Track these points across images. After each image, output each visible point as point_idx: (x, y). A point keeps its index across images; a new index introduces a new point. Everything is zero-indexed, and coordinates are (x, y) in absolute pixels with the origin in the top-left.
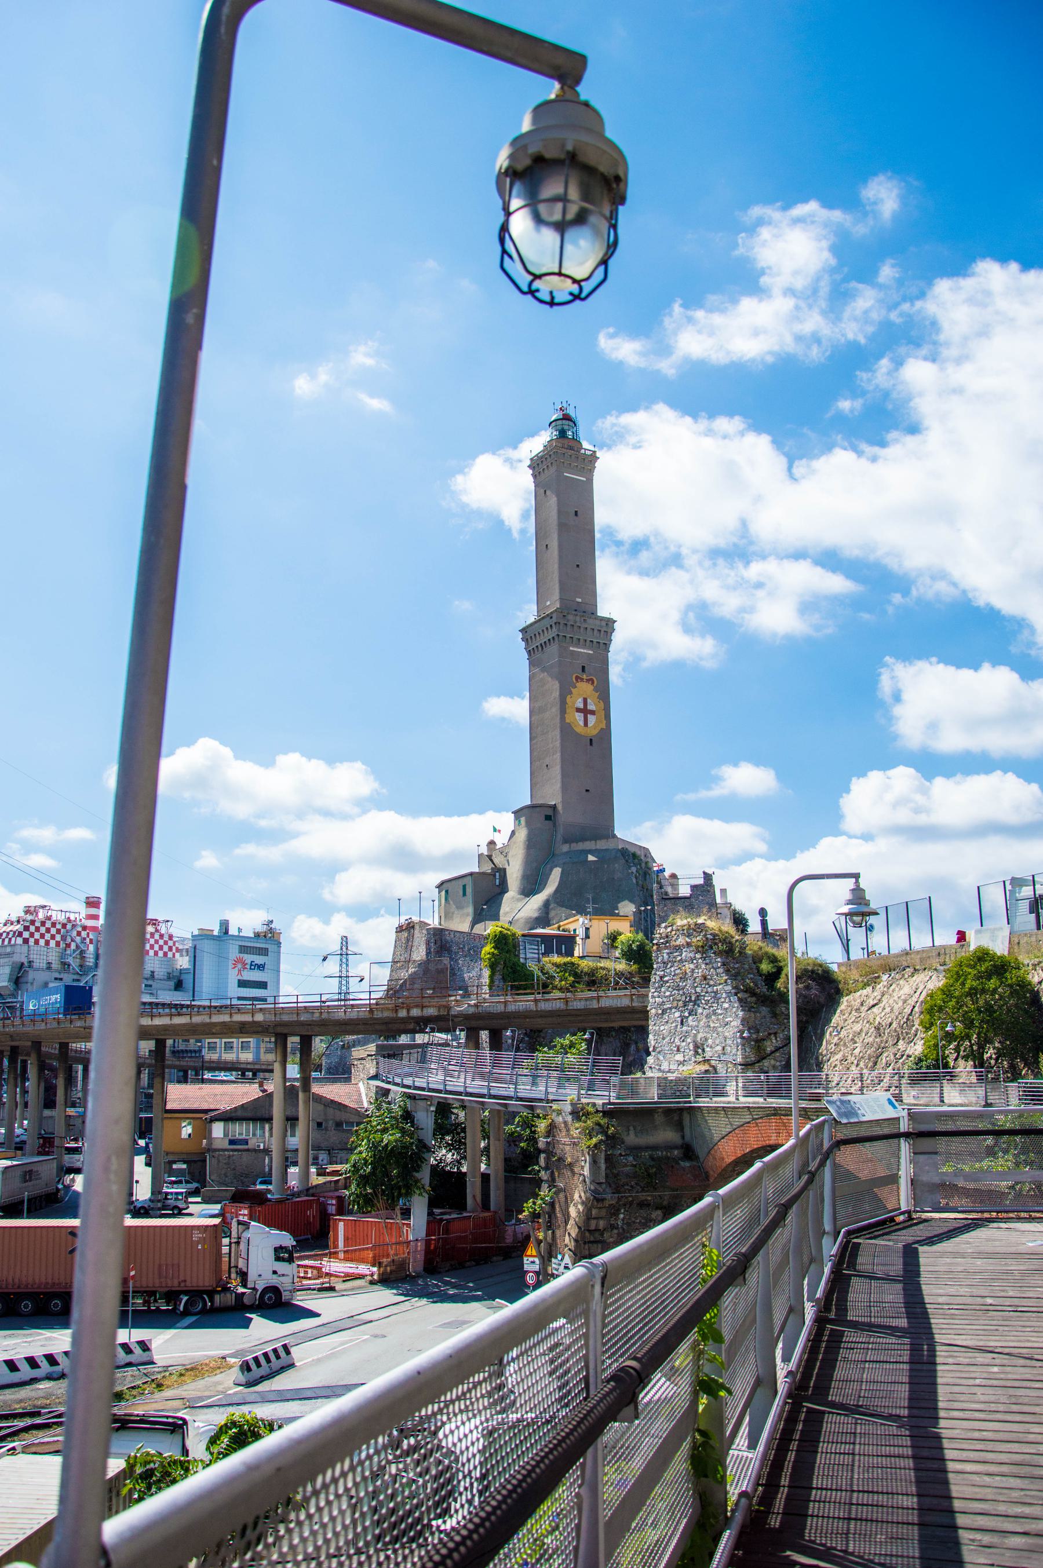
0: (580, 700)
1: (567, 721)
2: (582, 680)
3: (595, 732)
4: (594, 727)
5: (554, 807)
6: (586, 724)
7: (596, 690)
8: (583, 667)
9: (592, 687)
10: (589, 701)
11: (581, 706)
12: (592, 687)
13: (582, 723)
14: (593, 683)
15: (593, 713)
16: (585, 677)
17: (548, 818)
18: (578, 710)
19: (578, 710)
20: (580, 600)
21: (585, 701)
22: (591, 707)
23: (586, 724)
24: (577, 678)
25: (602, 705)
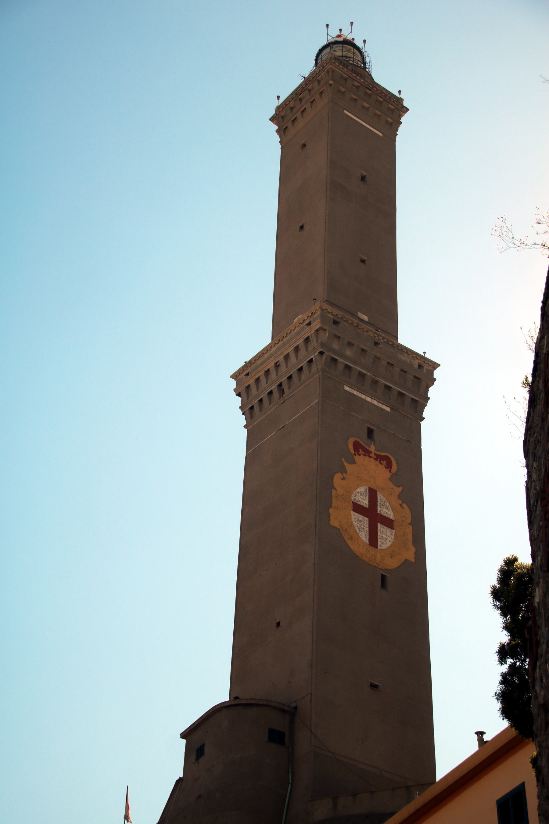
0: (362, 489)
1: (334, 522)
2: (367, 453)
3: (392, 563)
4: (392, 552)
7: (395, 479)
8: (370, 432)
10: (380, 497)
11: (365, 502)
12: (387, 474)
13: (364, 536)
14: (389, 466)
15: (389, 523)
16: (372, 448)
17: (276, 737)
18: (357, 508)
19: (357, 508)
20: (366, 318)
21: (373, 495)
22: (385, 510)
24: (357, 446)
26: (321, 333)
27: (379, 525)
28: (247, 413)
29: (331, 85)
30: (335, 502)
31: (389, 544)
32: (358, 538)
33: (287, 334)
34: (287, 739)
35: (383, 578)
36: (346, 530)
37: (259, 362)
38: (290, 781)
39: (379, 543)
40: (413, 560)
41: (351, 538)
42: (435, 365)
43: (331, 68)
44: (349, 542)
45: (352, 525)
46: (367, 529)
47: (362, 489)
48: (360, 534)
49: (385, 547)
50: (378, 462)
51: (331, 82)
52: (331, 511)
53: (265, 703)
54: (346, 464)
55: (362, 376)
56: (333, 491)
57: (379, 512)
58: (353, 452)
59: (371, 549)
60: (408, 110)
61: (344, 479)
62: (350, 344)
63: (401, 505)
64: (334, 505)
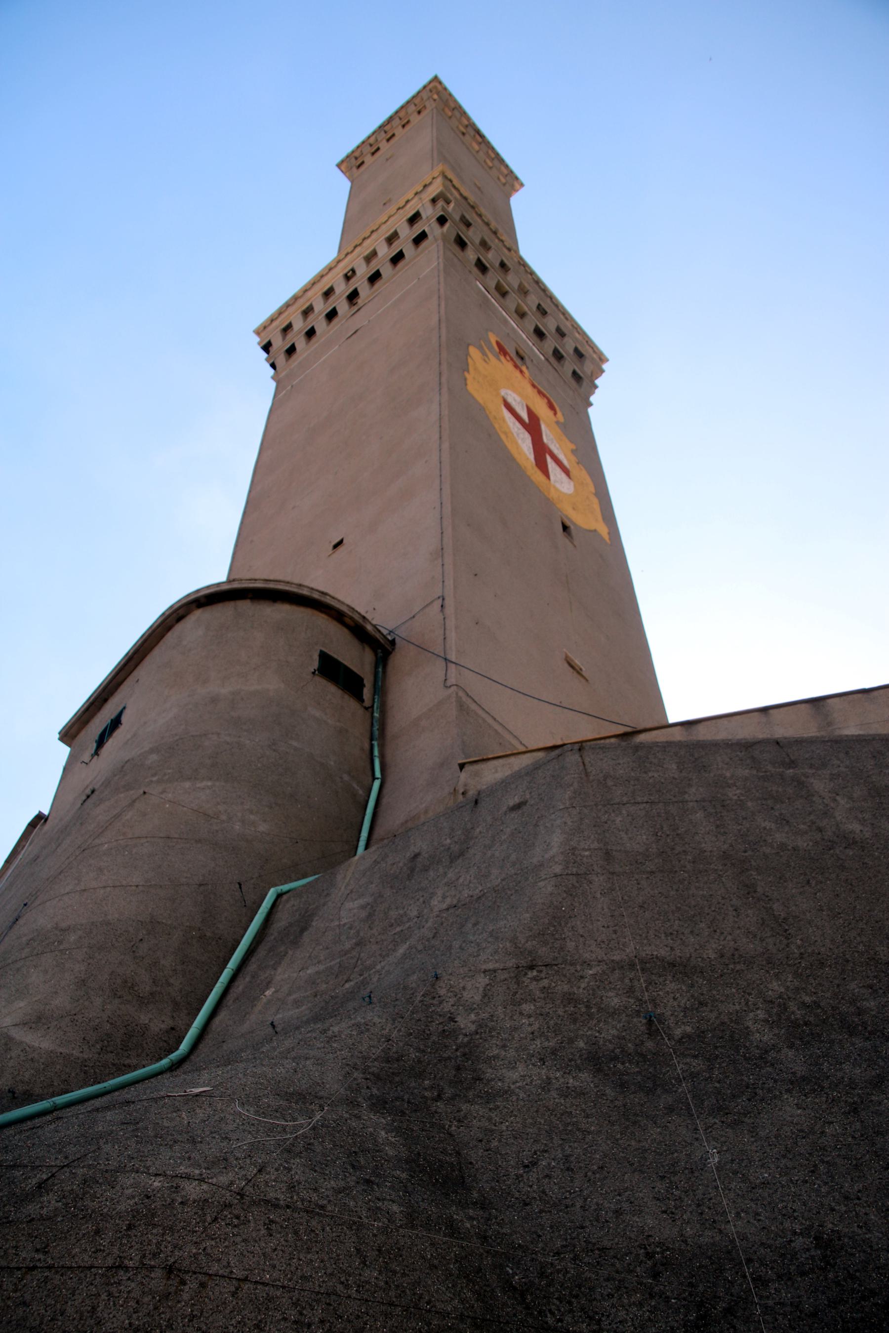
9: (554, 419)
11: (525, 416)
26: (441, 203)
28: (281, 360)
29: (435, 100)
32: (517, 443)
33: (372, 232)
34: (367, 693)
35: (565, 528)
37: (310, 294)
38: (378, 774)
39: (552, 477)
40: (608, 541)
42: (602, 359)
43: (435, 87)
44: (503, 437)
47: (518, 399)
51: (435, 97)
53: (316, 596)
56: (470, 360)
60: (522, 185)
63: (578, 463)
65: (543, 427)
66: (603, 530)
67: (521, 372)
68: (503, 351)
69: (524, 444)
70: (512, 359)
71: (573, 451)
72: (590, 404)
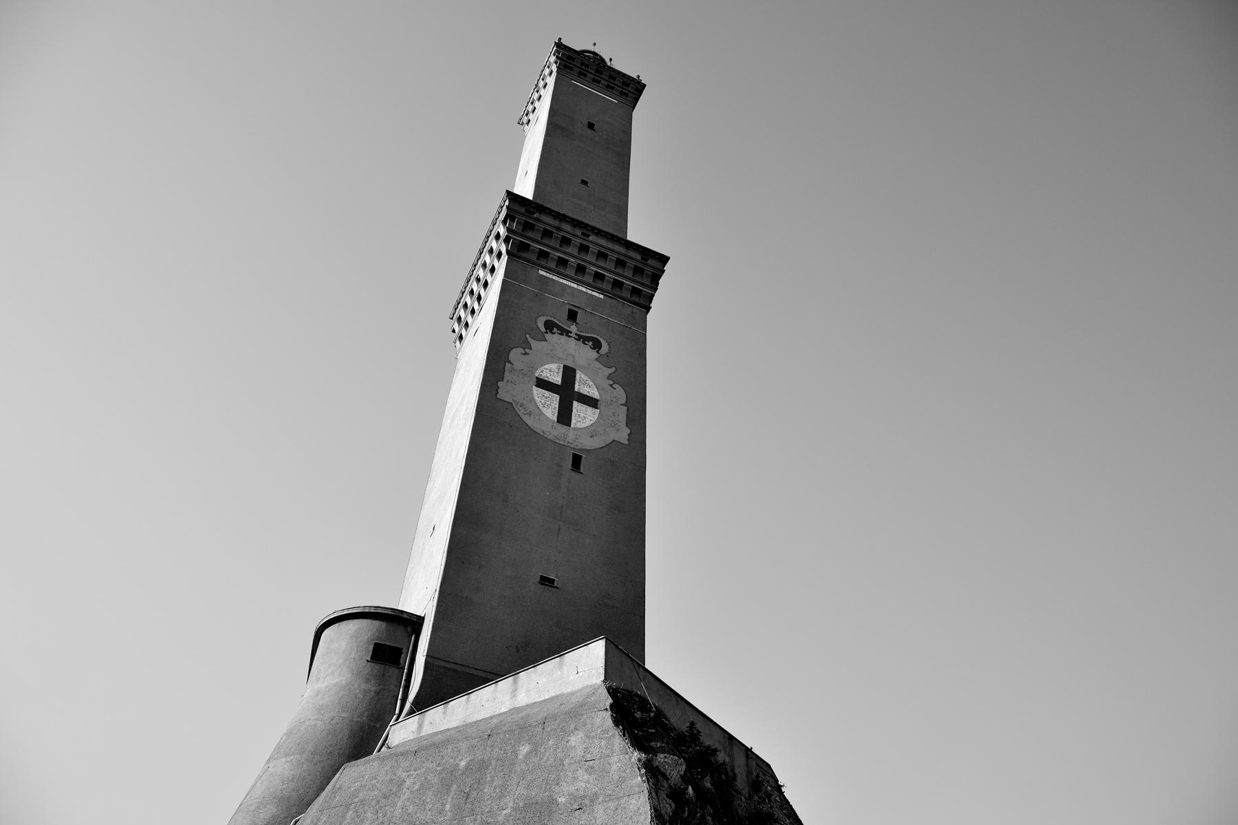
1: (501, 395)
2: (565, 332)
4: (592, 431)
5: (415, 623)
6: (565, 416)
7: (604, 360)
10: (579, 375)
11: (557, 379)
12: (594, 354)
14: (597, 345)
16: (573, 328)
18: (543, 384)
19: (543, 384)
21: (569, 374)
23: (565, 416)
24: (550, 326)
25: (620, 394)
27: (575, 404)
30: (507, 376)
31: (588, 423)
32: (541, 413)
35: (577, 461)
36: (522, 405)
39: (573, 421)
41: (530, 414)
42: (664, 259)
44: (525, 418)
45: (532, 400)
46: (556, 404)
47: (554, 366)
48: (544, 410)
49: (580, 425)
50: (580, 343)
52: (500, 384)
54: (530, 340)
55: (562, 262)
57: (577, 388)
58: (543, 330)
59: (562, 429)
61: (526, 354)
62: (547, 234)
64: (506, 378)
65: (578, 377)
66: (623, 435)
67: (566, 333)
68: (550, 326)
69: (549, 405)
70: (559, 328)
71: (608, 378)
72: (648, 309)
